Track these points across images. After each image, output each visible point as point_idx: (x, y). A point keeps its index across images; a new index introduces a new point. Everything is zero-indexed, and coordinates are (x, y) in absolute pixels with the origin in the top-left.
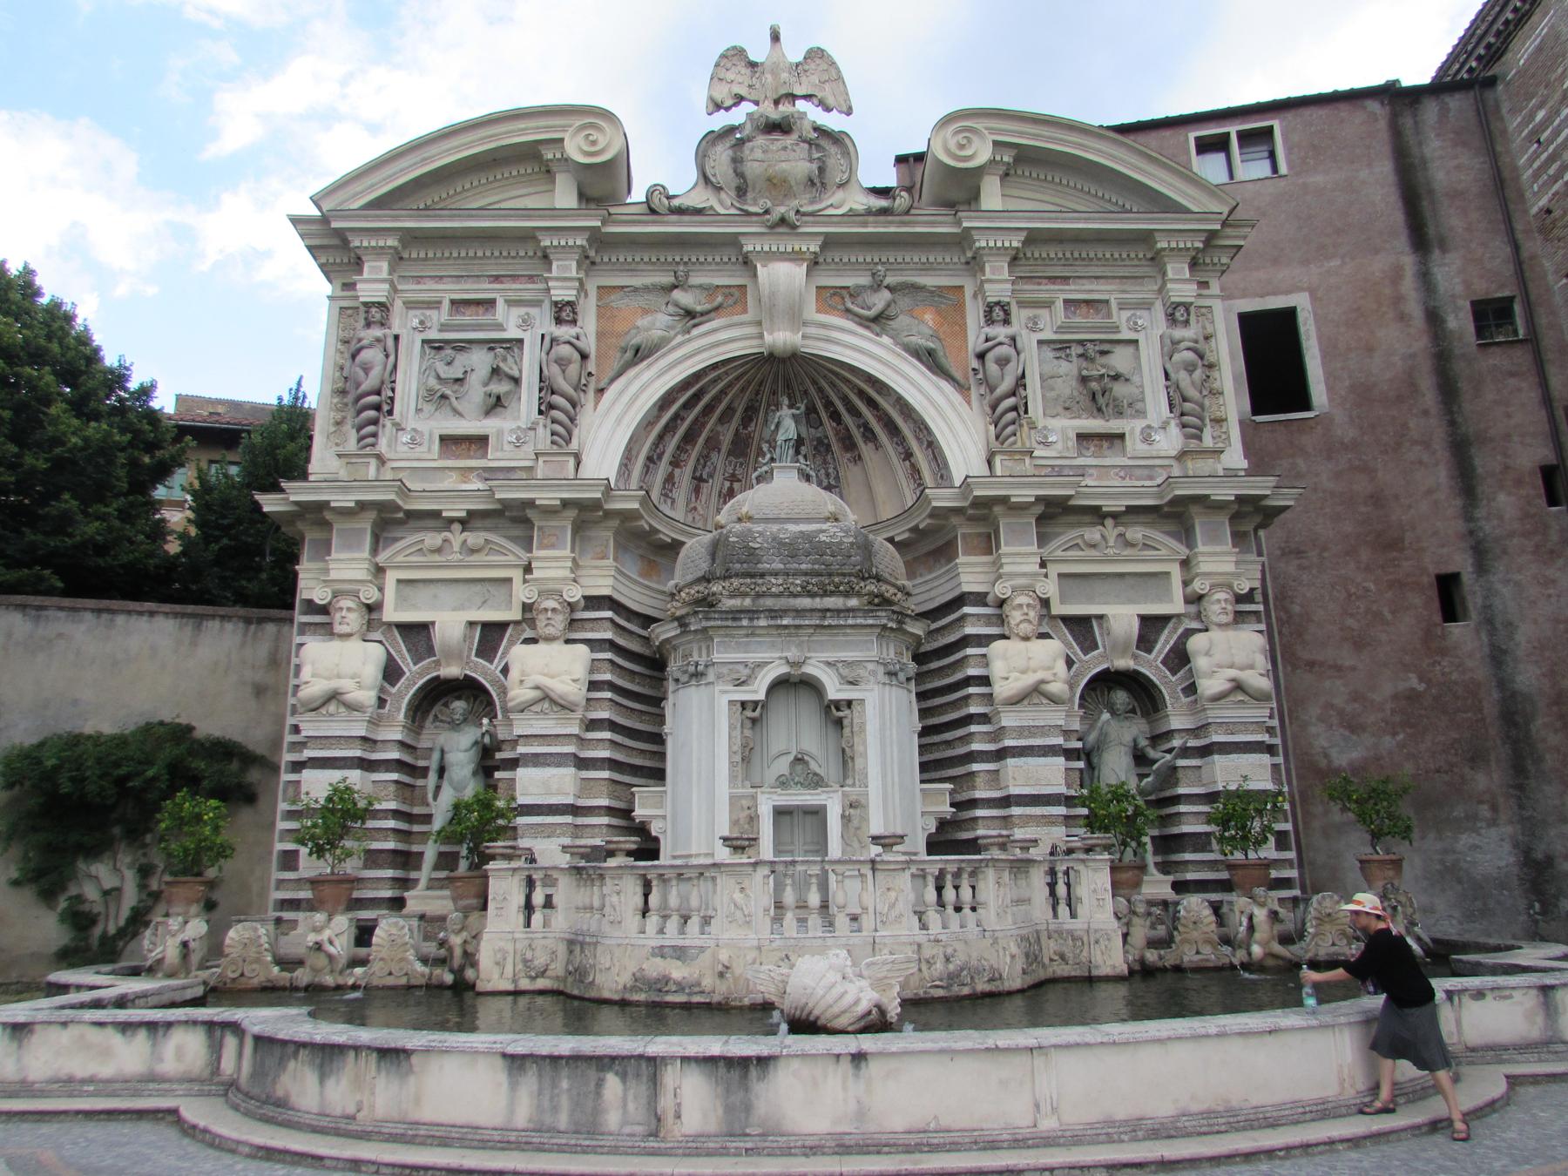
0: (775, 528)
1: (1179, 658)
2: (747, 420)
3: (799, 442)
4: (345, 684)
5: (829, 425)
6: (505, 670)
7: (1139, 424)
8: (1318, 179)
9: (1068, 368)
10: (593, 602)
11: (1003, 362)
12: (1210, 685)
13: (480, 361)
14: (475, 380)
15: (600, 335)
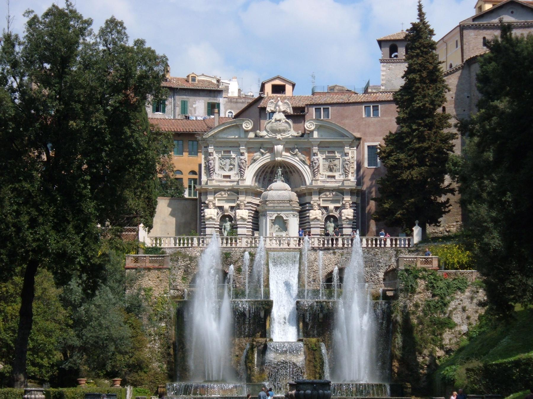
0: (277, 192)
1: (340, 213)
2: (273, 168)
3: (282, 174)
4: (212, 216)
5: (287, 169)
6: (235, 213)
7: (339, 173)
8: (385, 118)
9: (327, 163)
10: (248, 203)
11: (315, 163)
12: (343, 218)
13: (228, 161)
14: (227, 165)
15: (248, 156)
